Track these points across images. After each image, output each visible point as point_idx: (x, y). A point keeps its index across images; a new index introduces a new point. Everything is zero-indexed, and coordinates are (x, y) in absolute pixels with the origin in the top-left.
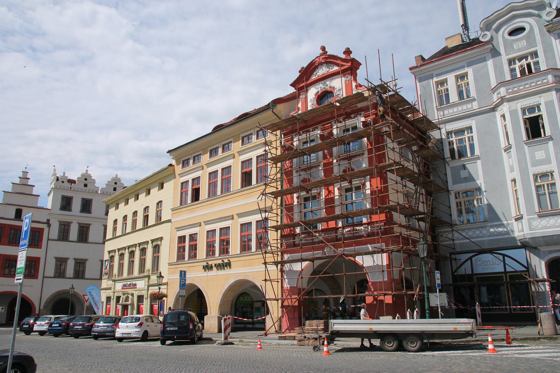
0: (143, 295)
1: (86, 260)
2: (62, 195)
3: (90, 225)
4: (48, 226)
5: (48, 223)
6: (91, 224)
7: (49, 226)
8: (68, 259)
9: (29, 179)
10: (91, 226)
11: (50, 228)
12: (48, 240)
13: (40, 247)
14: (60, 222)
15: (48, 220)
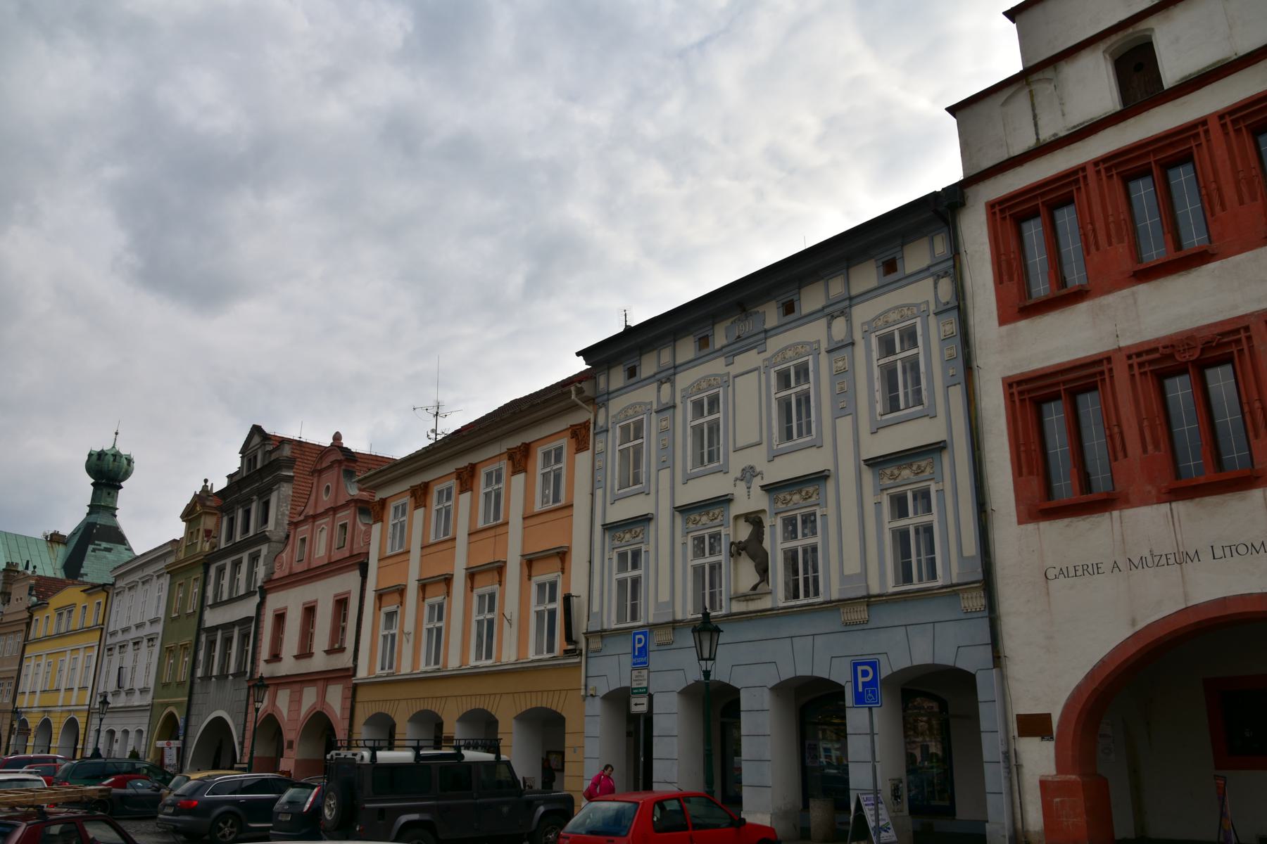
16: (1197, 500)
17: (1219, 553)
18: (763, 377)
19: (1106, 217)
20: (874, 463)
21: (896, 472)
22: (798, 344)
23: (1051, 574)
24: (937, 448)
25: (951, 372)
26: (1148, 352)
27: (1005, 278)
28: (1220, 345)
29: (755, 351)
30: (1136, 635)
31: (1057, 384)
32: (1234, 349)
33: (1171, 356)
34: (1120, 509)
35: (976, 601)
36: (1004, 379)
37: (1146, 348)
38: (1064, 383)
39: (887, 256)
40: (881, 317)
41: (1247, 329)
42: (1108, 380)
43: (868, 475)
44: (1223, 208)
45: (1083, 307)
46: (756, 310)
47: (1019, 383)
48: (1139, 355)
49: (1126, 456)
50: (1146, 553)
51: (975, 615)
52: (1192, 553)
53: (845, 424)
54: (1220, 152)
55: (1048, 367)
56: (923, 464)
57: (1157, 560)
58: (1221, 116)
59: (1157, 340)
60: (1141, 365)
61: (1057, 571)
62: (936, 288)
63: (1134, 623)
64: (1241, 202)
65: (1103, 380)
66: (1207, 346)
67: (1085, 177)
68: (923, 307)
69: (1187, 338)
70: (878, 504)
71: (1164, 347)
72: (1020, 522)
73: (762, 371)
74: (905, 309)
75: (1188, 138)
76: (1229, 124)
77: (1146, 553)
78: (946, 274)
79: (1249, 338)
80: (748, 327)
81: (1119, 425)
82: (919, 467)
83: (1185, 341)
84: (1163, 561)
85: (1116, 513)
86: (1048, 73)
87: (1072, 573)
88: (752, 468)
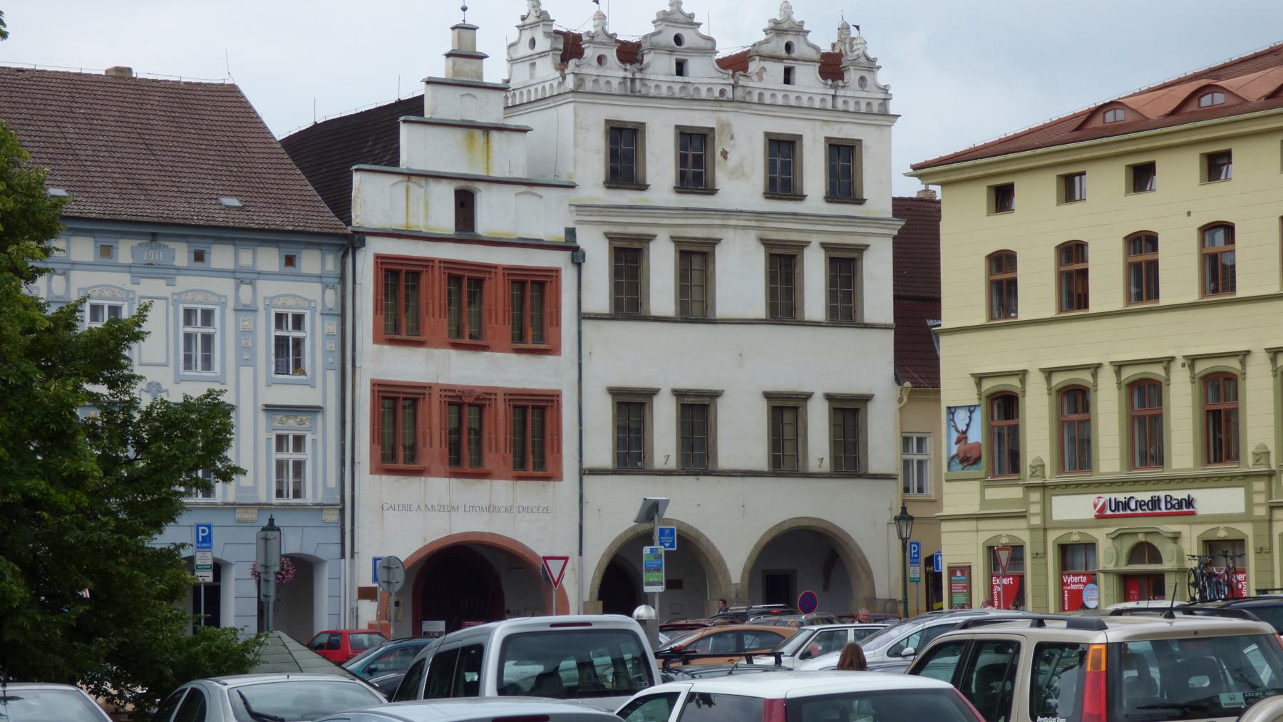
0: (1203, 541)
1: (715, 395)
2: (607, 121)
3: (714, 242)
4: (573, 262)
5: (570, 246)
6: (717, 241)
7: (578, 258)
8: (652, 393)
9: (481, 57)
10: (718, 249)
11: (584, 266)
12: (582, 317)
13: (554, 350)
14: (611, 237)
15: (571, 233)
16: (463, 479)
17: (467, 509)
18: (171, 308)
19: (440, 300)
20: (270, 409)
21: (284, 419)
22: (208, 292)
23: (386, 507)
24: (315, 410)
25: (330, 360)
26: (449, 390)
27: (379, 312)
28: (484, 399)
29: (164, 281)
30: (425, 547)
31: (399, 393)
32: (487, 402)
33: (460, 397)
34: (426, 476)
35: (333, 517)
36: (372, 380)
37: (450, 388)
38: (404, 393)
39: (290, 252)
40: (281, 298)
41: (495, 394)
42: (427, 399)
43: (262, 417)
44: (496, 323)
45: (421, 351)
46: (166, 243)
47: (379, 385)
48: (445, 390)
49: (431, 447)
50: (435, 504)
51: (331, 525)
52: (456, 507)
53: (246, 373)
54: (501, 289)
55: (398, 381)
56: (304, 418)
57: (441, 508)
58: (506, 268)
59: (456, 386)
60: (445, 396)
61: (389, 506)
62: (323, 294)
63: (425, 540)
64: (504, 324)
65: (424, 398)
66: (477, 398)
67: (432, 266)
68: (313, 305)
69: (471, 390)
70: (269, 439)
71: (459, 391)
72: (371, 473)
73: (170, 302)
74: (300, 300)
75: (485, 271)
76: (506, 275)
77: (435, 504)
78: (333, 288)
79: (495, 399)
80: (153, 255)
81: (430, 428)
82: (301, 421)
83: (469, 391)
84: (442, 509)
85: (423, 478)
86: (423, 181)
87: (397, 508)
88: (158, 384)
